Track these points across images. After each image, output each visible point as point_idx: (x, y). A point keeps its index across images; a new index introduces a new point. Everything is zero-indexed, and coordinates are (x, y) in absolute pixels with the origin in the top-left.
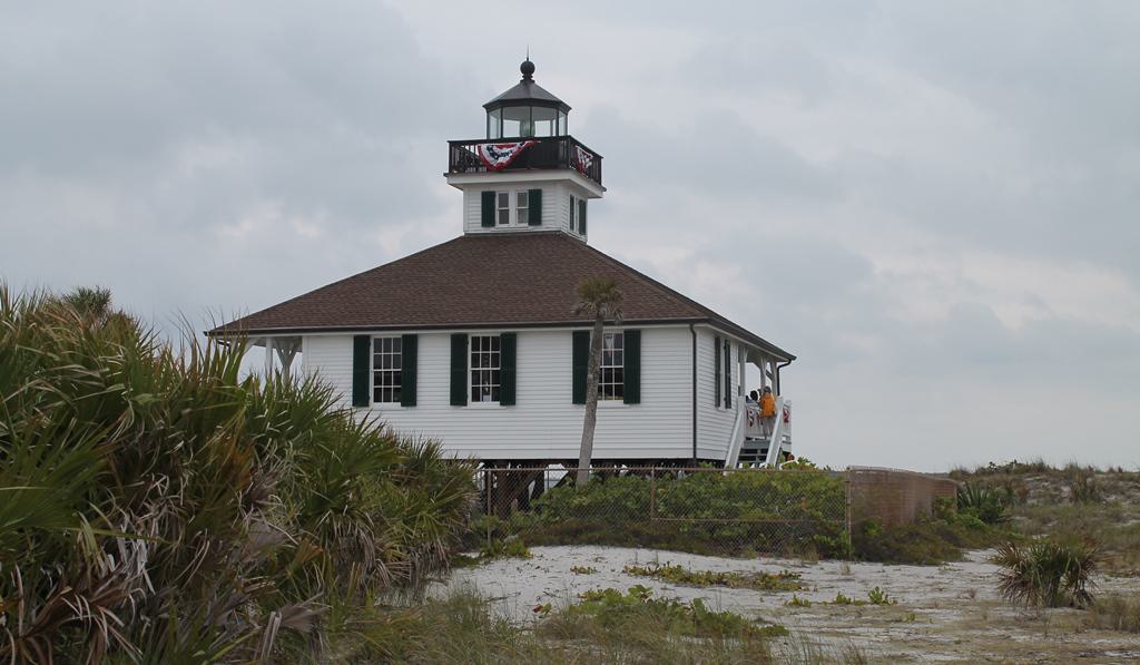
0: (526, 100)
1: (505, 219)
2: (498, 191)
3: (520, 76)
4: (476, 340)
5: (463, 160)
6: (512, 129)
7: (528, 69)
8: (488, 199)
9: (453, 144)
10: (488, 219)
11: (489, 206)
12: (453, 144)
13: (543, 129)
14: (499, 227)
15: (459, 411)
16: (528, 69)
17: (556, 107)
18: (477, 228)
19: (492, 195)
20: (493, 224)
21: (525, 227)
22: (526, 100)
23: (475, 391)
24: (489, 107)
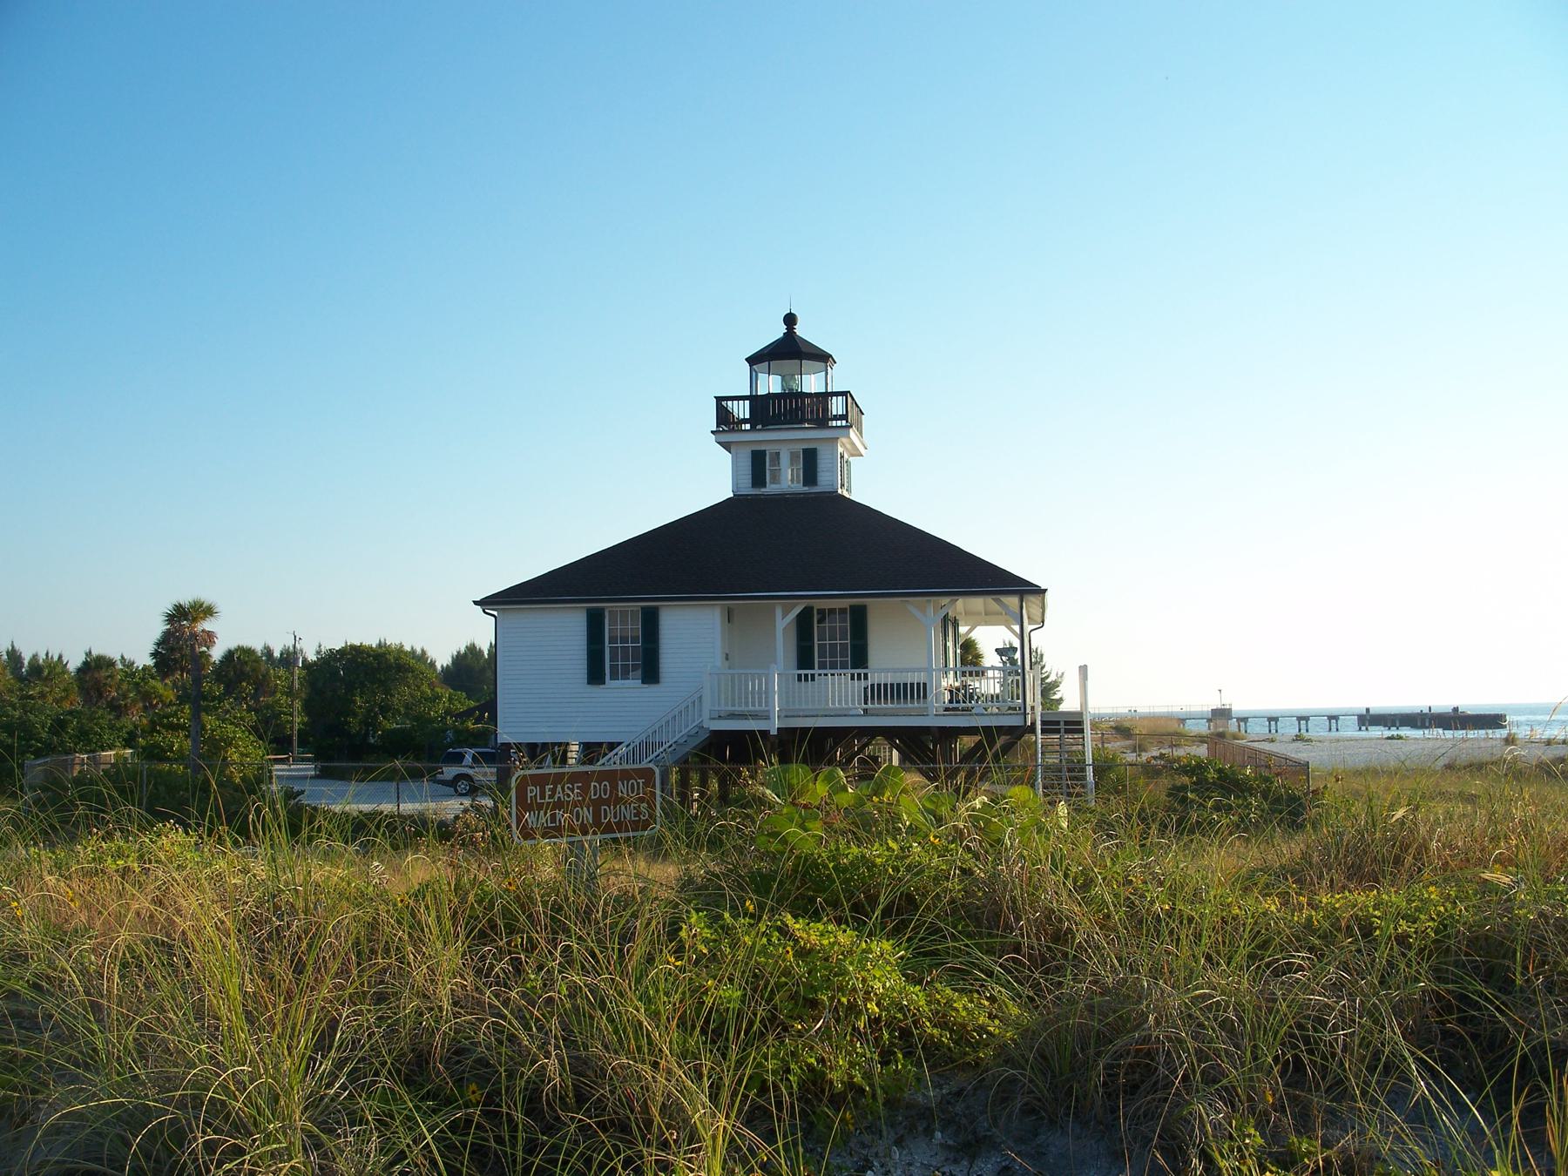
0: (789, 349)
1: (775, 480)
2: (770, 449)
3: (783, 329)
4: (821, 612)
5: (724, 418)
6: (770, 384)
7: (790, 320)
8: (758, 459)
9: (719, 399)
10: (758, 478)
11: (759, 465)
12: (719, 399)
13: (812, 383)
14: (771, 488)
15: (596, 690)
16: (790, 320)
17: (823, 358)
18: (747, 489)
19: (763, 453)
20: (764, 485)
21: (799, 487)
22: (789, 349)
23: (614, 669)
24: (753, 360)
